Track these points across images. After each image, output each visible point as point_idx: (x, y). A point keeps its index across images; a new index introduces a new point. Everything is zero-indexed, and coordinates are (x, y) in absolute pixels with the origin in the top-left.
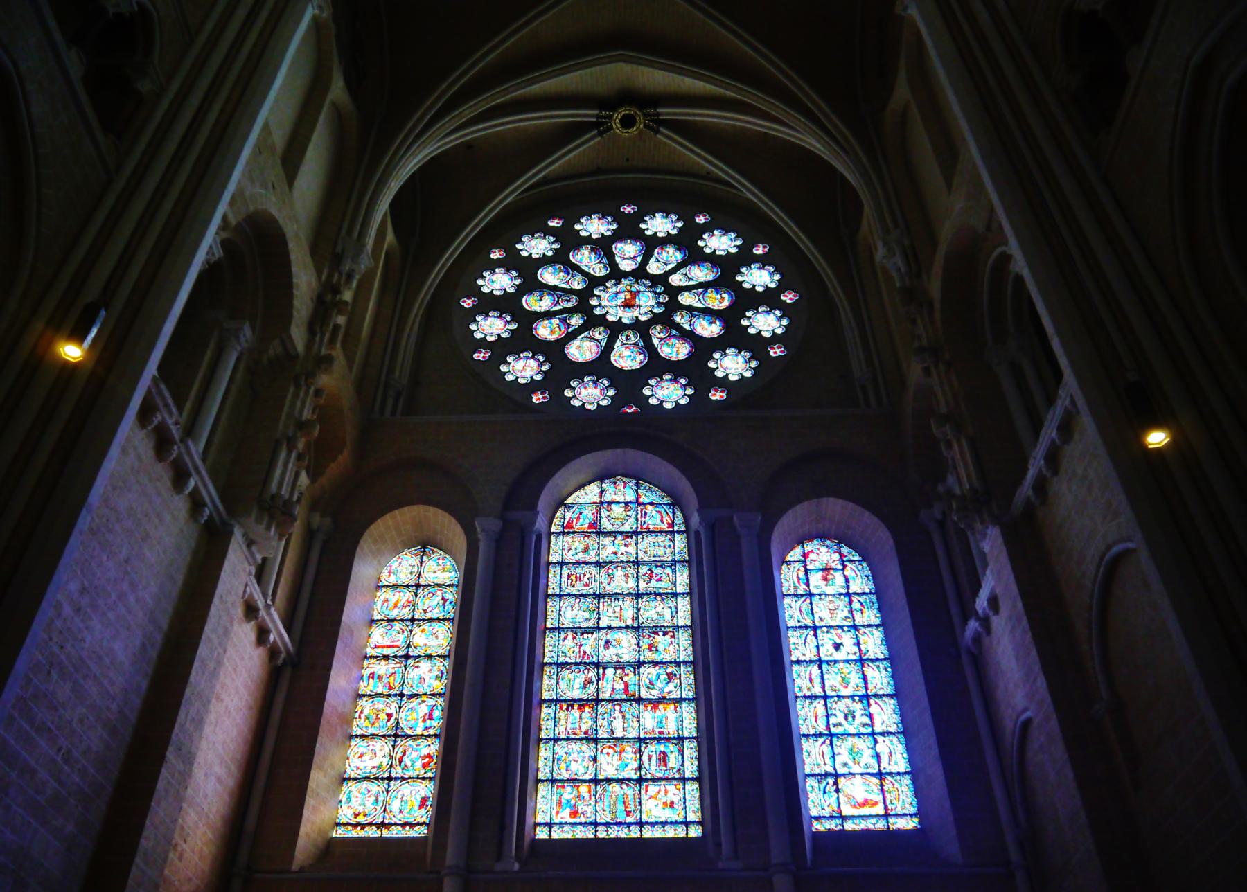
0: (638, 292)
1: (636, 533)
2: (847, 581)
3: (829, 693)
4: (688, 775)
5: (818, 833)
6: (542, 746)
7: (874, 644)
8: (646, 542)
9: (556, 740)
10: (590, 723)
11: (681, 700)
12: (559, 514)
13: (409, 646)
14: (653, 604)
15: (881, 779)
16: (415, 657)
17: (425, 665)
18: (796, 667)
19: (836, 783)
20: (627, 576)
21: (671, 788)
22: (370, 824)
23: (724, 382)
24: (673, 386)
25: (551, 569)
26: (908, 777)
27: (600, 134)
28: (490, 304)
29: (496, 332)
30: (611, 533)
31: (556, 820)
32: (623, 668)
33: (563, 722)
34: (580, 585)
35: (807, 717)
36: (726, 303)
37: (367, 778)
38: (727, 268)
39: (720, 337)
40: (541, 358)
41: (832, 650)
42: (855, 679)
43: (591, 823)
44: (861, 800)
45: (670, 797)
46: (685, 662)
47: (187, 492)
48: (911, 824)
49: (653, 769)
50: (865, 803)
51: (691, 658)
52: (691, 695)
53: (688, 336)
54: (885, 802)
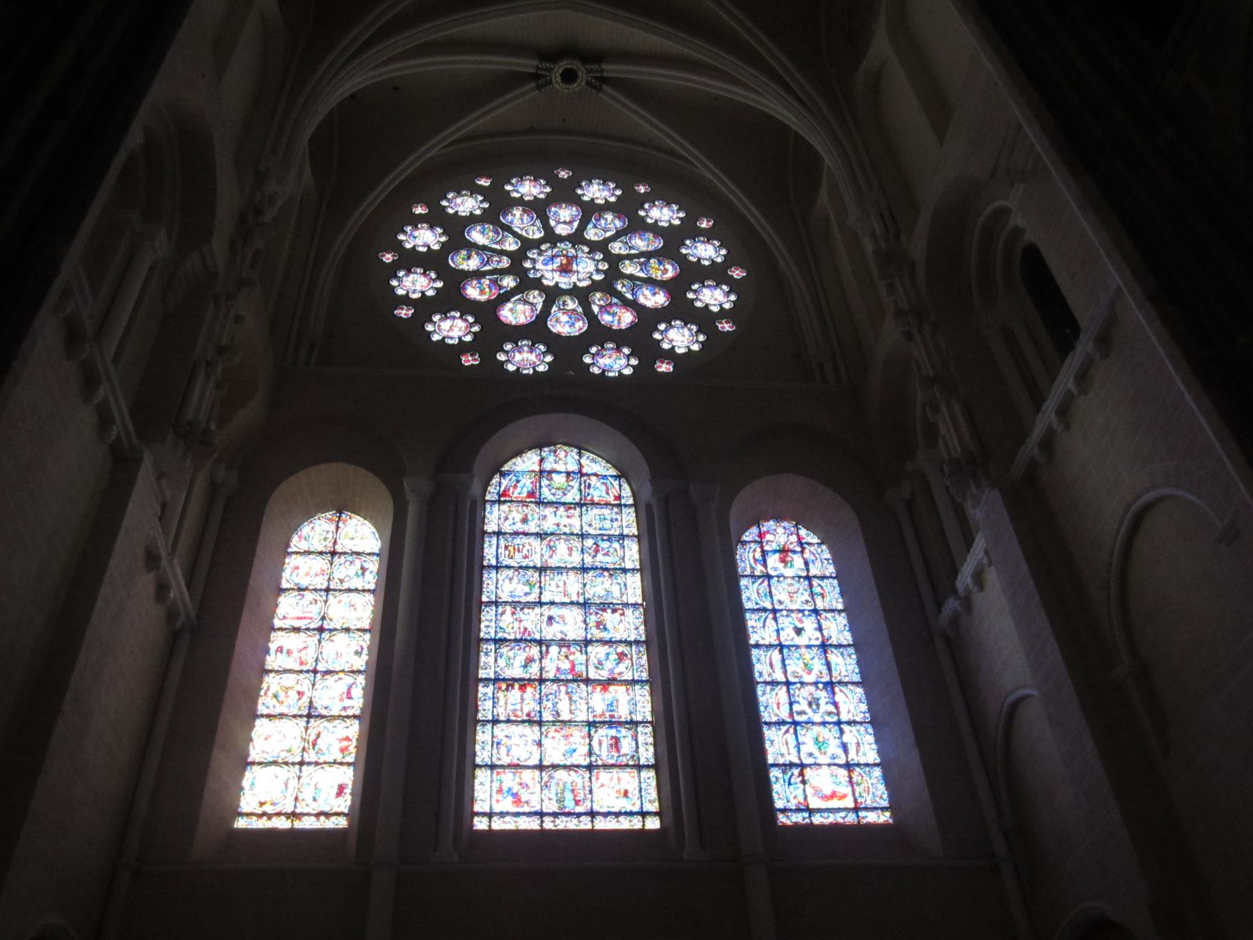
1: (580, 505)
2: (806, 564)
3: (792, 679)
6: (479, 728)
7: (838, 629)
9: (495, 722)
11: (633, 682)
12: (495, 481)
13: (323, 618)
14: (600, 580)
15: (850, 771)
16: (331, 631)
17: (341, 638)
19: (801, 774)
20: (570, 549)
22: (279, 814)
23: (670, 355)
25: (487, 539)
27: (538, 87)
28: (411, 260)
29: (419, 288)
30: (551, 503)
31: (497, 809)
32: (569, 647)
34: (518, 557)
35: (772, 704)
36: (670, 274)
37: (275, 763)
38: (672, 241)
39: (663, 308)
40: (471, 319)
41: (793, 634)
42: (818, 665)
43: (536, 813)
44: (828, 792)
45: (623, 786)
47: (96, 401)
48: (884, 818)
50: (833, 796)
52: (645, 676)
53: (633, 305)
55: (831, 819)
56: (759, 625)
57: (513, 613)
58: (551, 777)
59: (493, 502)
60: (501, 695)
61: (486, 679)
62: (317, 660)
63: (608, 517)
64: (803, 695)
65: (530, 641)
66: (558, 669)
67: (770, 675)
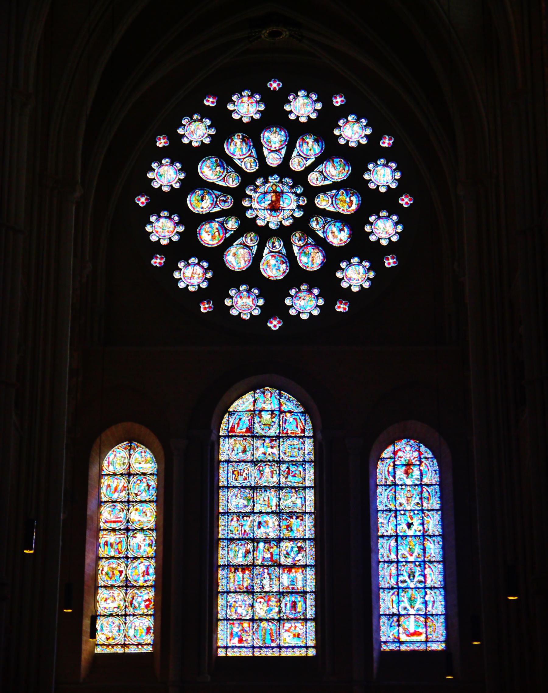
0: (282, 192)
1: (278, 437)
2: (421, 475)
3: (401, 559)
4: (308, 616)
5: (385, 652)
6: (219, 596)
7: (434, 524)
8: (286, 445)
9: (228, 593)
10: (249, 581)
11: (305, 566)
12: (225, 420)
13: (128, 522)
16: (133, 530)
17: (140, 536)
18: (381, 540)
19: (398, 621)
20: (272, 472)
21: (299, 625)
22: (117, 644)
24: (309, 297)
26: (443, 617)
31: (230, 645)
33: (232, 581)
34: (241, 478)
35: (386, 575)
37: (111, 615)
41: (405, 527)
42: (418, 550)
44: (412, 631)
46: (309, 539)
48: (440, 647)
49: (287, 611)
51: (313, 537)
52: (312, 562)
53: (321, 243)
54: (426, 633)
55: (412, 647)
56: (385, 521)
57: (238, 520)
58: (259, 626)
59: (225, 437)
60: (231, 575)
61: (223, 565)
63: (296, 447)
64: (405, 570)
65: (247, 539)
66: (264, 558)
67: (388, 557)
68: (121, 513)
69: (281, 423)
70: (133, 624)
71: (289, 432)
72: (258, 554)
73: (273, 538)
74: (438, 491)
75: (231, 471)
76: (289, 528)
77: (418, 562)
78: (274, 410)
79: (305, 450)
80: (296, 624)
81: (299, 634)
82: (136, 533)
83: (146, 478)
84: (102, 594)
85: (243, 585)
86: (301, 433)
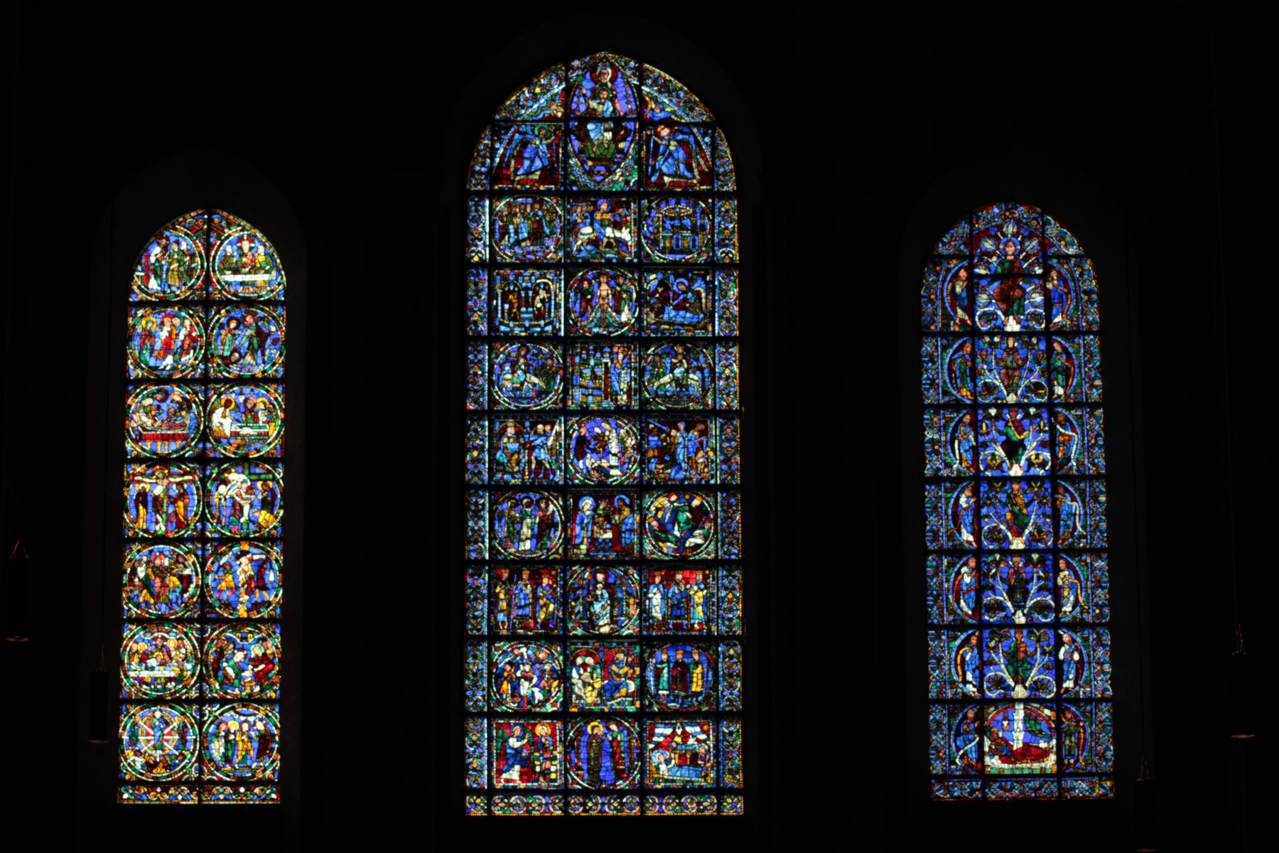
1: (632, 195)
2: (1048, 304)
7: (1081, 445)
9: (493, 637)
19: (980, 716)
20: (617, 297)
22: (177, 783)
33: (503, 605)
34: (526, 313)
41: (1000, 452)
44: (1017, 745)
50: (1030, 753)
54: (1059, 754)
57: (519, 434)
62: (203, 519)
63: (687, 222)
66: (593, 541)
68: (184, 413)
69: (643, 154)
70: (223, 727)
71: (667, 179)
72: (578, 529)
73: (621, 485)
74: (1095, 350)
75: (499, 291)
76: (667, 454)
77: (1038, 551)
78: (624, 118)
79: (712, 234)
80: (689, 729)
81: (695, 756)
82: (226, 470)
83: (254, 314)
84: (136, 640)
85: (535, 618)
86: (701, 183)
